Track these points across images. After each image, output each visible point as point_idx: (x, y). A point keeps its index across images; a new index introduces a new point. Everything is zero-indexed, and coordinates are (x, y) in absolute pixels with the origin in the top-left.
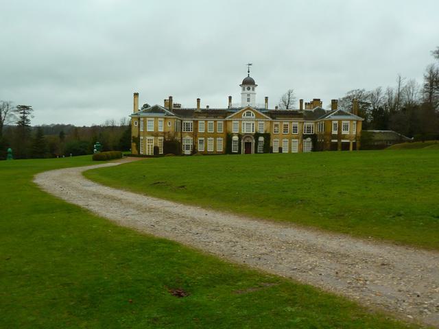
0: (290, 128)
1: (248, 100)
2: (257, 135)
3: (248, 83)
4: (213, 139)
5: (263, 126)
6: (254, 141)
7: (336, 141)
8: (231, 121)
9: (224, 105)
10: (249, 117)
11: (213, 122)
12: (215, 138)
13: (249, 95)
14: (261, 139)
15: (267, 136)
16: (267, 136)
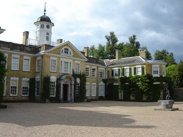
0: (90, 71)
1: (48, 39)
2: (75, 76)
3: (45, 21)
4: (17, 79)
5: (80, 66)
6: (73, 82)
7: (158, 83)
8: (49, 57)
9: (19, 40)
10: (66, 55)
11: (19, 56)
12: (21, 78)
13: (48, 34)
14: (78, 80)
15: (83, 77)
16: (83, 77)
